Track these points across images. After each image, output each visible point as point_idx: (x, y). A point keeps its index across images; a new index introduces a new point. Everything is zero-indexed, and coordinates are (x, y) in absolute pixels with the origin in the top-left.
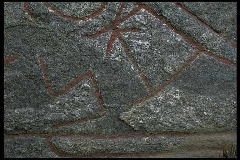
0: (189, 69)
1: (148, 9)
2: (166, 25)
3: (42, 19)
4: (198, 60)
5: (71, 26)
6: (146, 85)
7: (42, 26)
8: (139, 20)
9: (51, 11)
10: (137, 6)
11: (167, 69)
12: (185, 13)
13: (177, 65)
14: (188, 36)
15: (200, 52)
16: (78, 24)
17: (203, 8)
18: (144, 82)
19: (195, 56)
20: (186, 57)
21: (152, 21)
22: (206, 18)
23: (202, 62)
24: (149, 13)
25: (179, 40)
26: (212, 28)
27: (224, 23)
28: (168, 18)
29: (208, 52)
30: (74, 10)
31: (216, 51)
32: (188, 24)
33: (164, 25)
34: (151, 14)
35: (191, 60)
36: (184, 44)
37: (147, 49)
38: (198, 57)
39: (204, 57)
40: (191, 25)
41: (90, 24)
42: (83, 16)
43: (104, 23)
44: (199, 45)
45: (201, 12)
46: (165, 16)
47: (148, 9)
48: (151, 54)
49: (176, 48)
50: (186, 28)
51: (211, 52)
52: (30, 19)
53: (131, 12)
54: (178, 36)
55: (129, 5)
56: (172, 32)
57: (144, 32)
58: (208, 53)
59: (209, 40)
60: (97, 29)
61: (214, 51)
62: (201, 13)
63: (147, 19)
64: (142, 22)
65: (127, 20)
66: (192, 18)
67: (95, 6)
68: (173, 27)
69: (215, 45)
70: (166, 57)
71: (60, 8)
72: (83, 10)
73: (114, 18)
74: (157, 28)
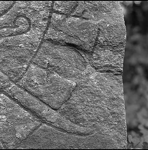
0: (34, 135)
1: (5, 94)
2: (18, 104)
4: (41, 129)
6: (4, 147)
11: (18, 135)
12: (31, 97)
13: (25, 133)
14: (33, 112)
15: (43, 124)
17: (42, 93)
18: (3, 145)
19: (39, 127)
20: (32, 127)
22: (45, 99)
23: (44, 130)
24: (7, 97)
25: (27, 115)
26: (50, 107)
27: (58, 103)
28: (19, 100)
29: (49, 123)
31: (53, 123)
32: (32, 104)
34: (8, 98)
35: (35, 129)
36: (30, 118)
37: (4, 121)
38: (41, 127)
39: (45, 127)
40: (35, 104)
44: (42, 119)
45: (42, 95)
47: (5, 94)
48: (7, 125)
49: (25, 121)
50: (31, 107)
51: (51, 123)
54: (26, 112)
56: (22, 109)
57: (3, 110)
58: (49, 124)
59: (47, 115)
61: (52, 123)
62: (41, 96)
63: (4, 101)
66: (35, 100)
68: (22, 106)
69: (53, 119)
70: (17, 127)
74: (11, 107)
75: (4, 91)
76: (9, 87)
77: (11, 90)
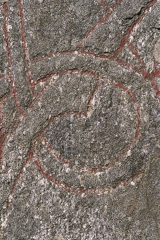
3: (141, 164)
5: (149, 130)
7: (148, 164)
8: (143, 43)
9: (129, 153)
10: (126, 45)
16: (146, 121)
21: (145, 26)
28: (142, 6)
30: (129, 125)
33: (152, 11)
41: (147, 105)
42: (137, 114)
43: (147, 88)
46: (140, 9)
52: (139, 179)
53: (133, 54)
55: (125, 55)
60: (153, 96)
64: (146, 39)
65: (143, 58)
67: (125, 98)
71: (126, 142)
72: (130, 114)
73: (141, 76)
75: (124, 35)
76: (117, 23)
77: (123, 21)
